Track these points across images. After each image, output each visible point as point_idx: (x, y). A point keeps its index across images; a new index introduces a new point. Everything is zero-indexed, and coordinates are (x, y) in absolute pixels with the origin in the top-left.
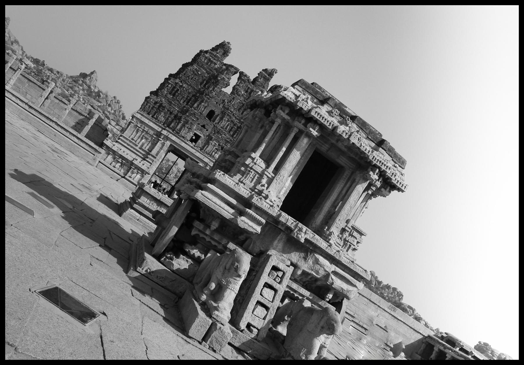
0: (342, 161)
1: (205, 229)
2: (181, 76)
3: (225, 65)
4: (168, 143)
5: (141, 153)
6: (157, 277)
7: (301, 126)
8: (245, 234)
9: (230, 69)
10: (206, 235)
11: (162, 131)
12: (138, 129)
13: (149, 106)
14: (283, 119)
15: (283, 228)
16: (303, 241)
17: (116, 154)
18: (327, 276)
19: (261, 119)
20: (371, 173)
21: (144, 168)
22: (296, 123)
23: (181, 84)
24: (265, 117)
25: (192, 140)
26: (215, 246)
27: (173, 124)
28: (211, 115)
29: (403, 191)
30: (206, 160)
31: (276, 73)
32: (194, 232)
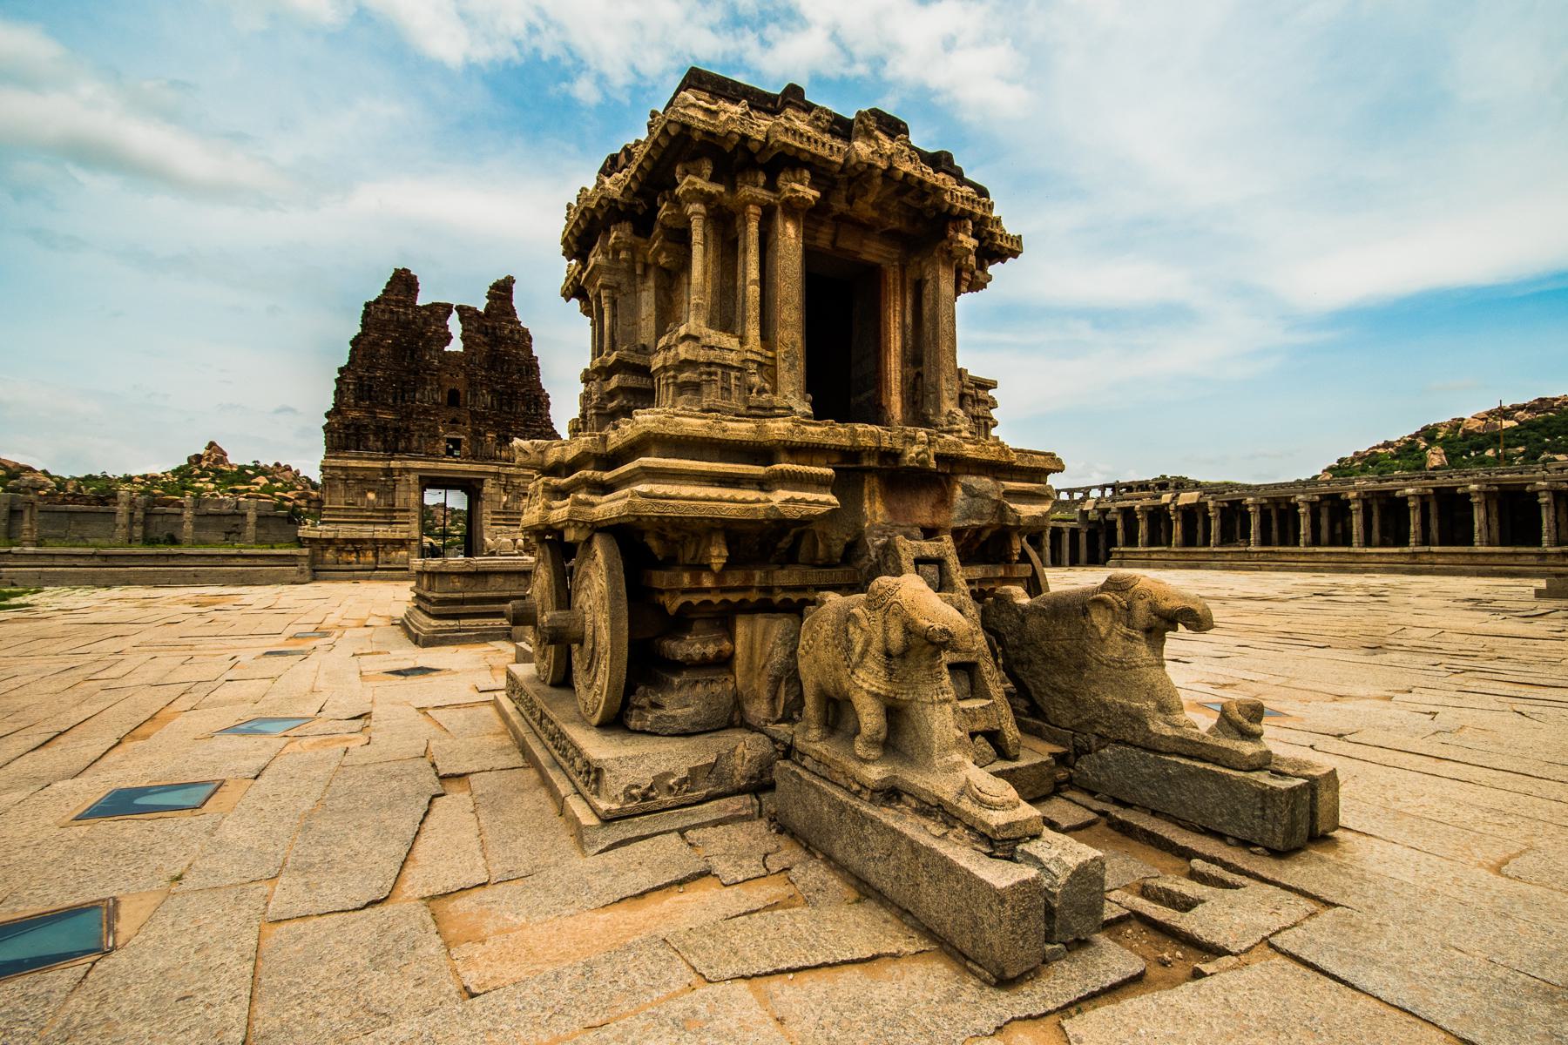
0: (873, 251)
1: (696, 578)
4: (413, 477)
6: (670, 789)
8: (793, 531)
10: (708, 591)
14: (707, 199)
15: (873, 463)
16: (933, 464)
18: (1000, 508)
19: (632, 249)
20: (961, 237)
22: (746, 191)
24: (642, 240)
25: (449, 452)
26: (743, 601)
27: (402, 444)
28: (454, 398)
29: (1015, 254)
30: (492, 469)
32: (673, 604)
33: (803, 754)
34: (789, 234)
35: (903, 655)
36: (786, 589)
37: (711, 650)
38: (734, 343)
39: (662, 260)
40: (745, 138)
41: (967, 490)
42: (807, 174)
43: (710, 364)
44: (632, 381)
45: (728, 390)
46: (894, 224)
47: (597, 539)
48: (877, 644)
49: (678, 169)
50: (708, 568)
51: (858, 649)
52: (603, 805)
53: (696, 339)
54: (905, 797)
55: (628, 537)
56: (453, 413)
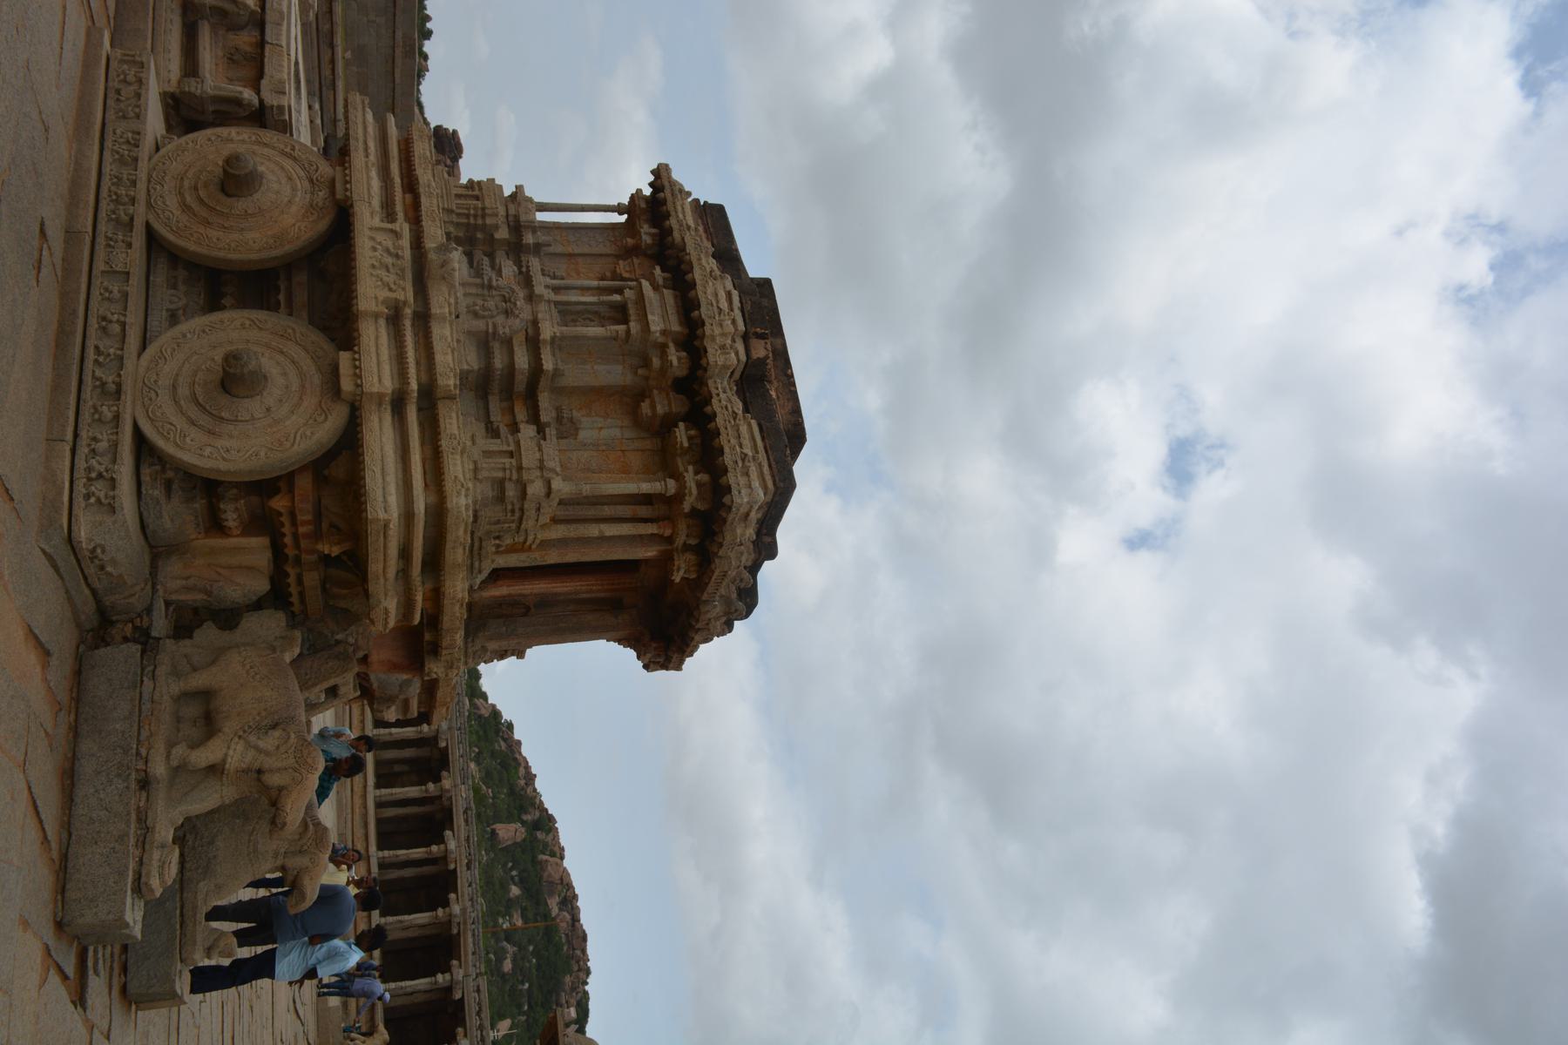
6: (102, 568)
7: (680, 540)
14: (678, 498)
19: (663, 371)
35: (259, 780)
37: (231, 524)
39: (645, 407)
40: (721, 545)
41: (408, 683)
42: (693, 576)
43: (522, 510)
45: (498, 522)
48: (269, 763)
50: (317, 535)
51: (261, 744)
52: (83, 533)
53: (548, 494)
54: (144, 794)
55: (349, 443)
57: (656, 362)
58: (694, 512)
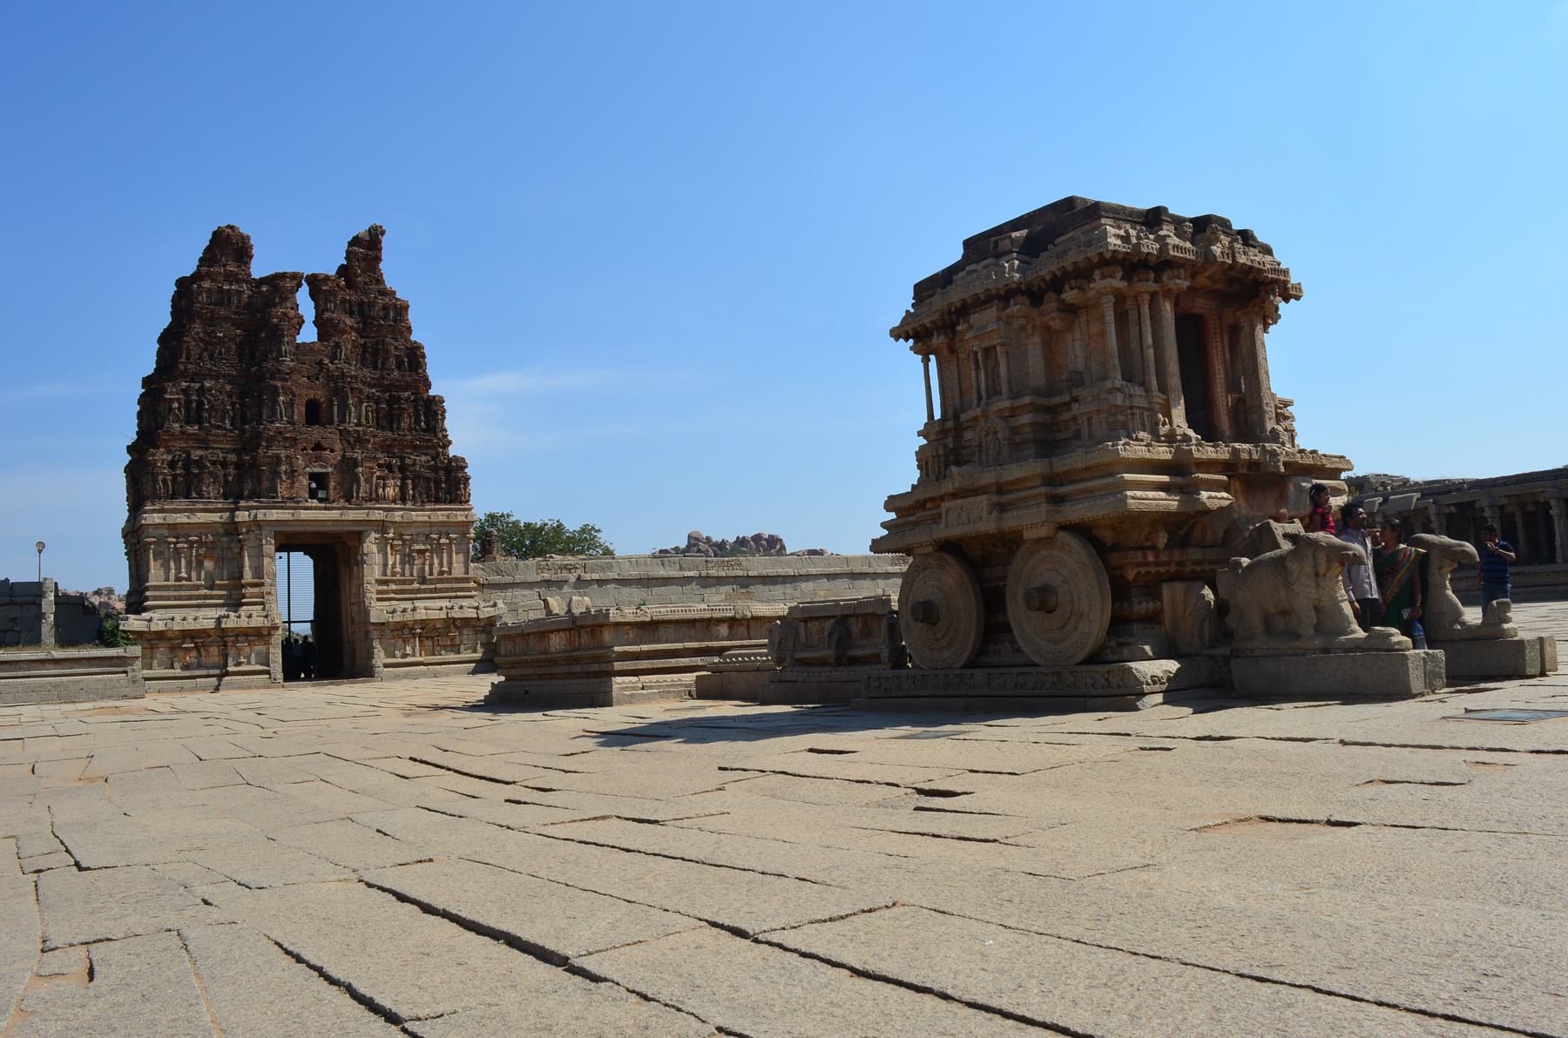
1: (1145, 556)
2: (181, 367)
3: (263, 281)
5: (220, 597)
7: (1152, 286)
9: (280, 286)
10: (1148, 564)
11: (233, 517)
12: (176, 549)
13: (165, 481)
17: (169, 635)
21: (258, 621)
23: (197, 386)
27: (248, 487)
28: (314, 414)
29: (1298, 298)
30: (378, 515)
31: (383, 233)
33: (1252, 650)
34: (1167, 309)
36: (1194, 563)
38: (1139, 391)
44: (1039, 418)
46: (1218, 286)
47: (1061, 534)
49: (1097, 272)
50: (1154, 548)
53: (1119, 390)
56: (316, 433)
57: (1022, 321)
58: (1127, 277)
